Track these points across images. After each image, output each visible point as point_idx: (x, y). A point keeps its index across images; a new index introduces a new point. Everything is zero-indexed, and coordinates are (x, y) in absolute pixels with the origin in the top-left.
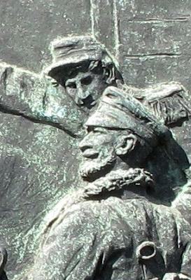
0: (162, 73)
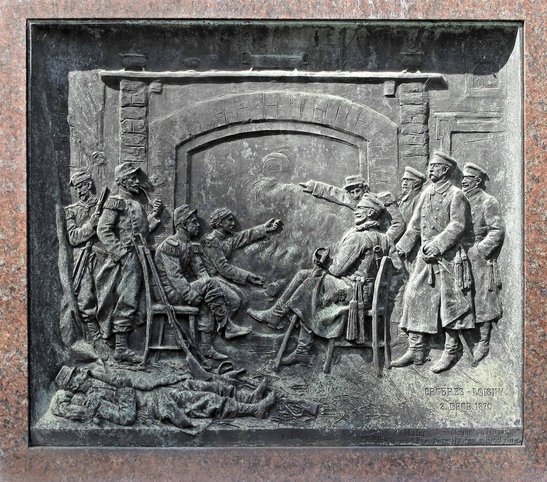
0: (384, 188)
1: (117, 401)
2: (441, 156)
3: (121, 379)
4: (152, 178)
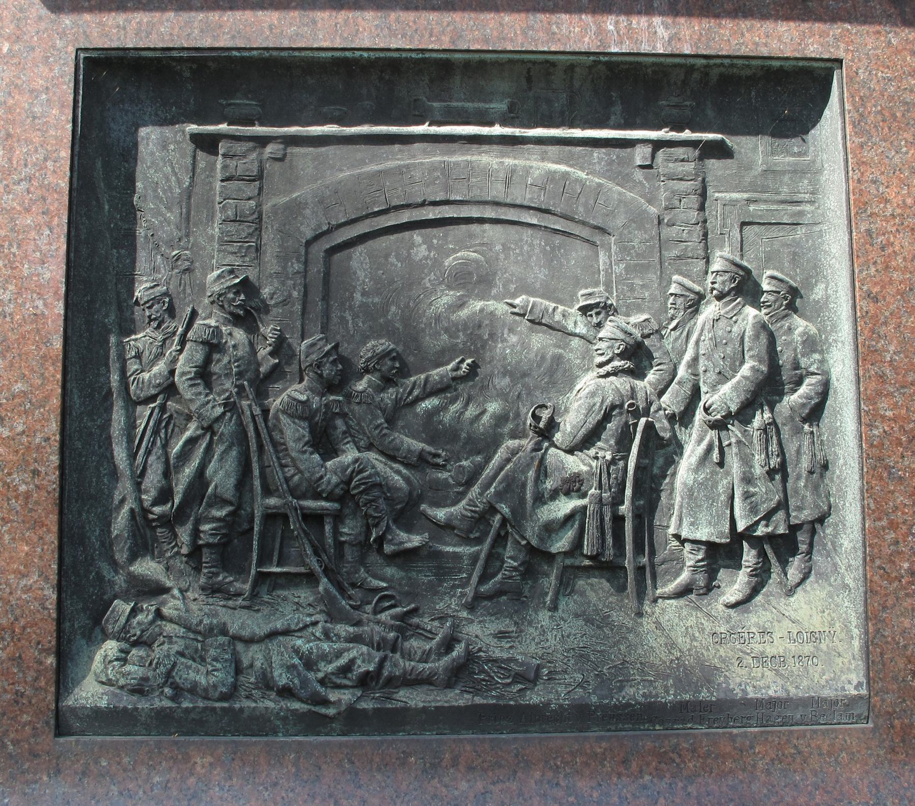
0: (639, 309)
1: (203, 660)
2: (727, 260)
3: (211, 623)
4: (266, 292)
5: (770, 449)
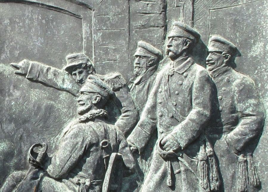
0: (112, 68)
2: (181, 27)
5: (211, 175)
